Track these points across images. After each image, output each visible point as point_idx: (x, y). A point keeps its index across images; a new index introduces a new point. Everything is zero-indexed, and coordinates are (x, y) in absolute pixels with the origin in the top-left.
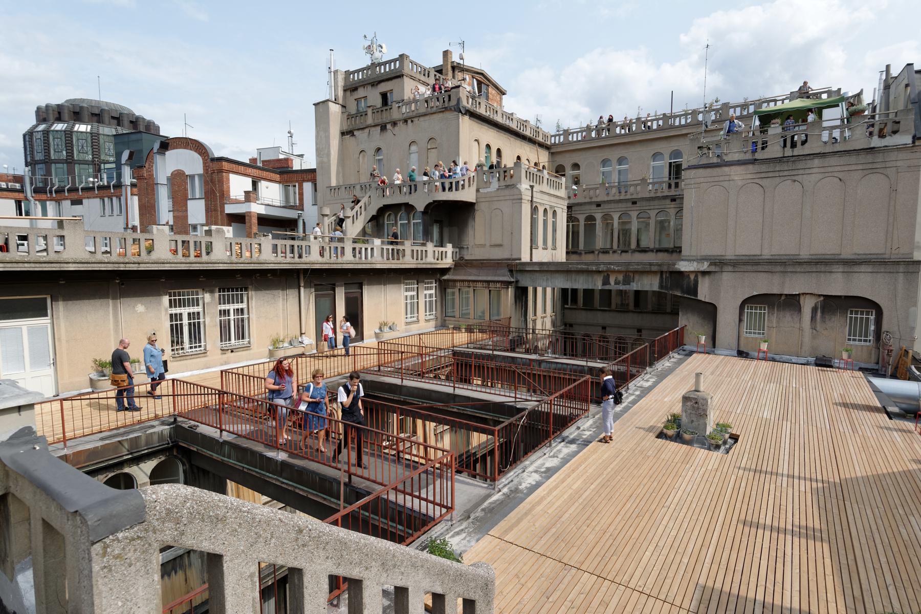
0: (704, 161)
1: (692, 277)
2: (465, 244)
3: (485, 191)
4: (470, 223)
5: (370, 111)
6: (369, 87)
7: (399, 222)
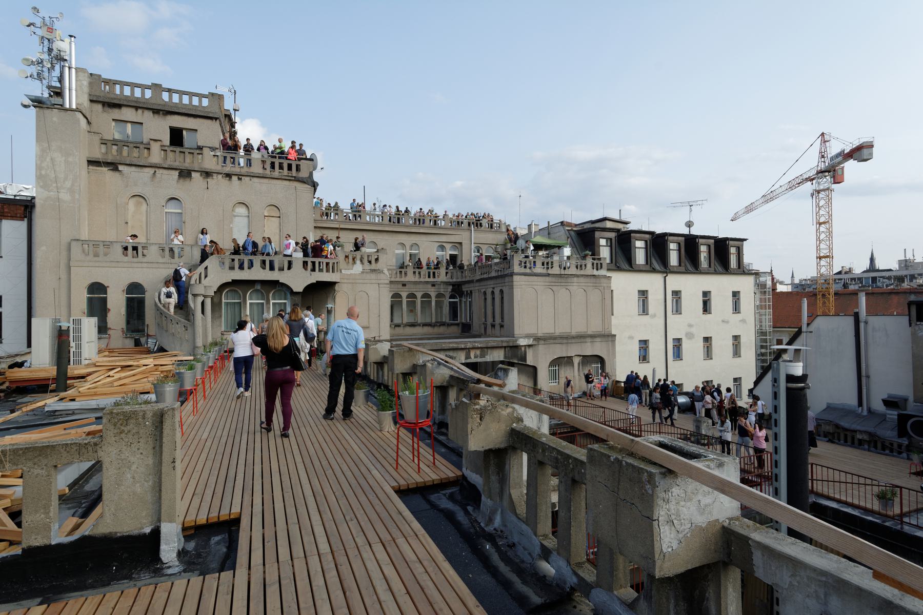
0: (523, 270)
1: (523, 349)
6: (148, 114)
7: (248, 302)
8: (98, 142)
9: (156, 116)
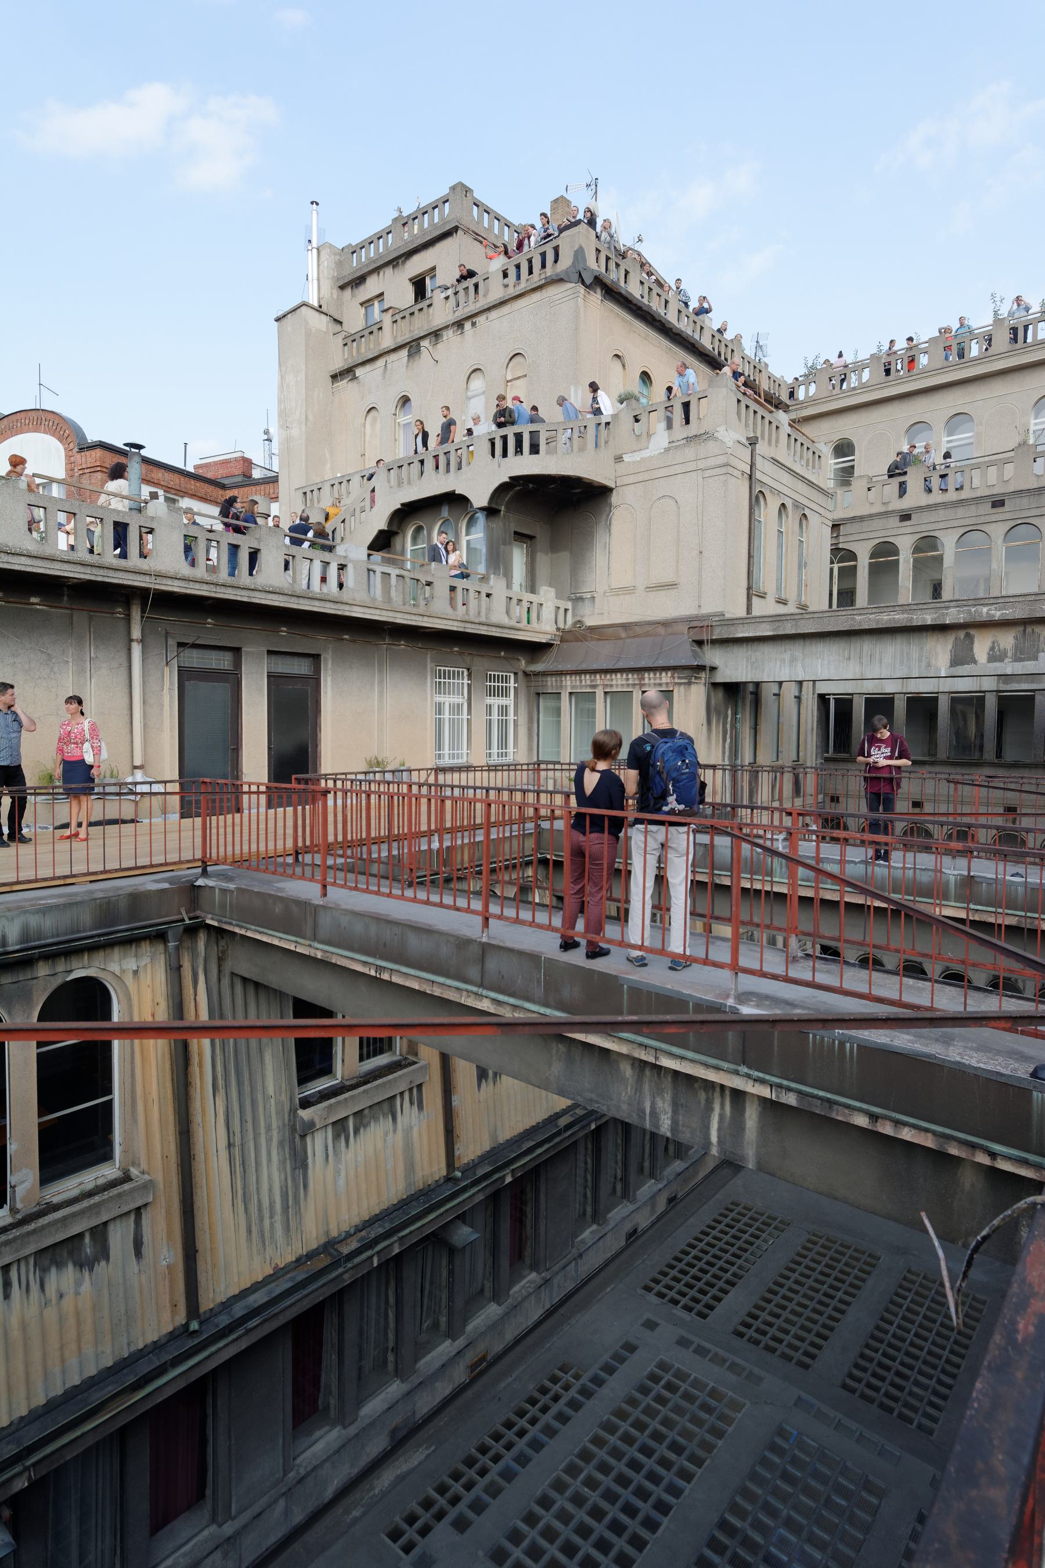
2: (585, 590)
3: (637, 457)
4: (600, 537)
5: (387, 319)
6: (389, 271)
8: (341, 342)
9: (396, 270)
